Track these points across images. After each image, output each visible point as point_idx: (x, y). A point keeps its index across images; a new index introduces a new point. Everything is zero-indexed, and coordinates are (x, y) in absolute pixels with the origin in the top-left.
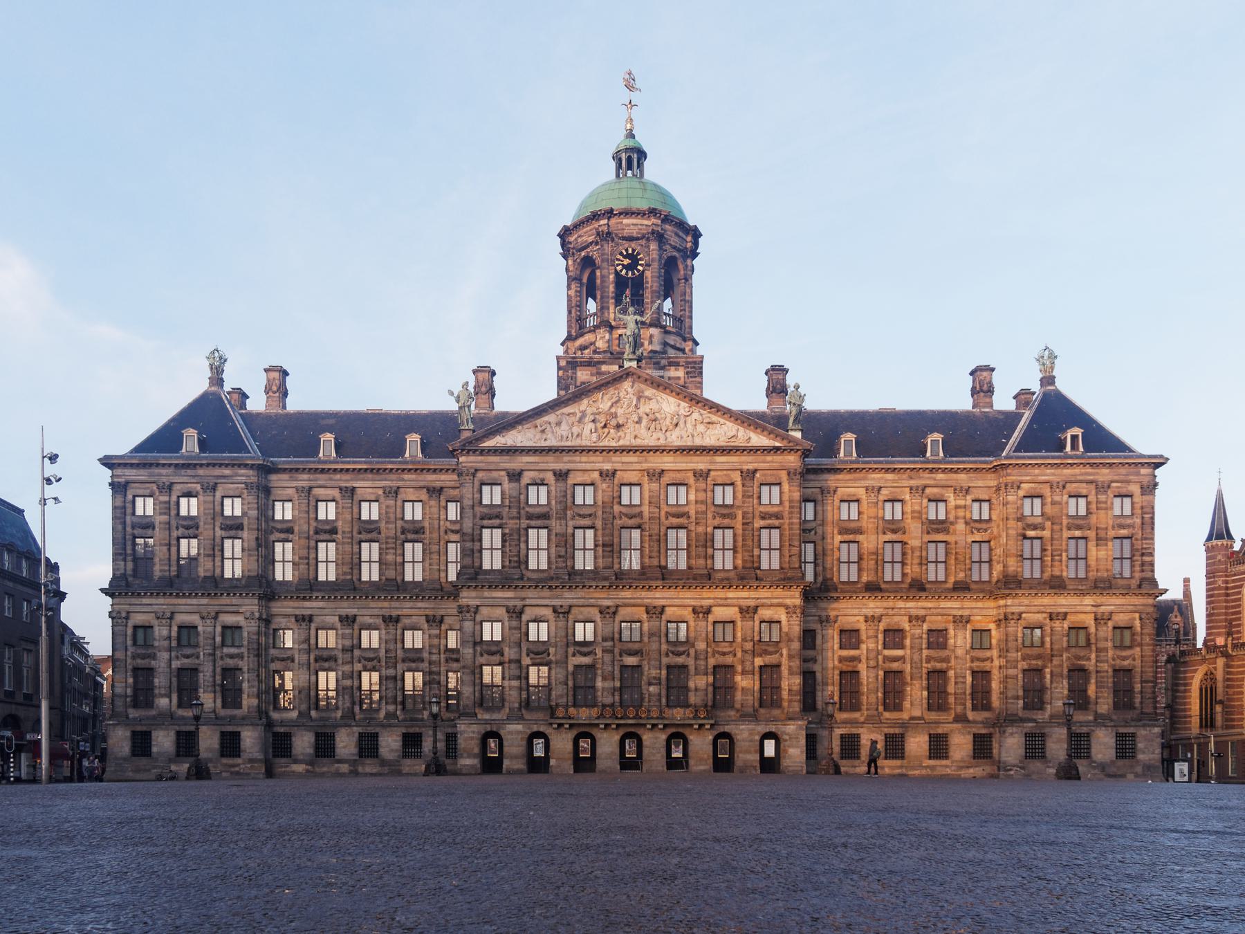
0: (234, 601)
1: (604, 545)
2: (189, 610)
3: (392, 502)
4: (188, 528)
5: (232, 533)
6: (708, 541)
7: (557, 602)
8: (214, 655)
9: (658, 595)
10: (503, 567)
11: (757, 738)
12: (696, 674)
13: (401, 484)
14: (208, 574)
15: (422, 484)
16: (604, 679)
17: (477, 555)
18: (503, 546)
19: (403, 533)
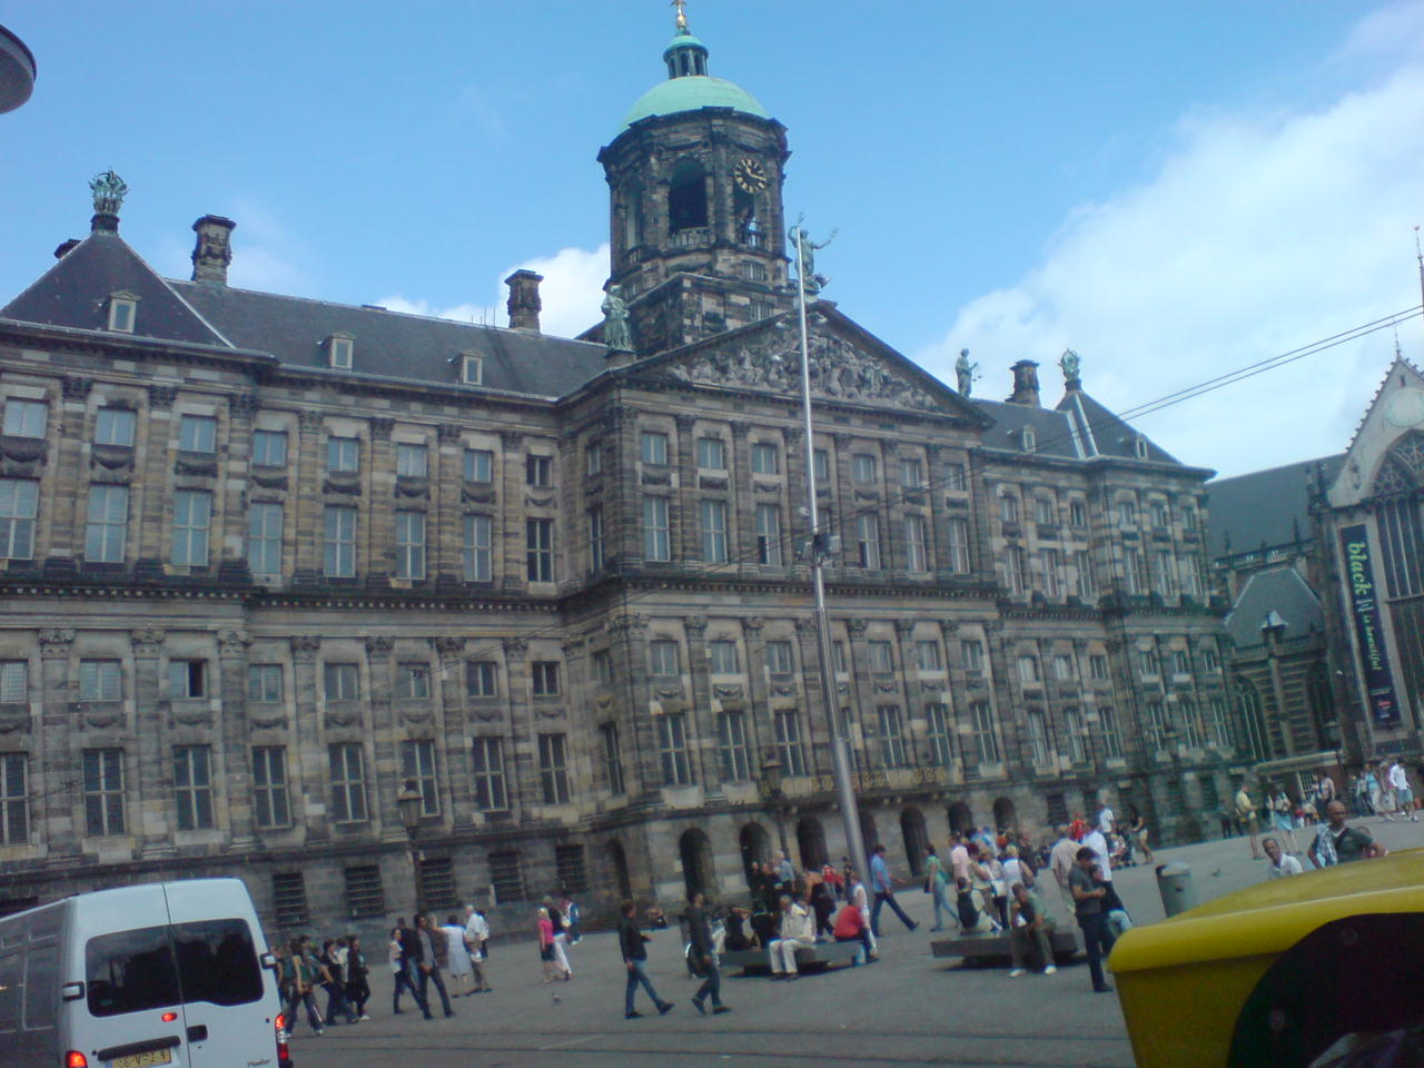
0: (198, 609)
1: (793, 531)
2: (103, 626)
3: (448, 450)
4: (111, 465)
5: (196, 481)
6: (902, 536)
7: (748, 612)
8: (156, 717)
9: (858, 602)
10: (673, 557)
11: (990, 808)
12: (910, 718)
13: (464, 422)
14: (148, 555)
15: (497, 425)
16: (812, 729)
17: (640, 536)
18: (671, 525)
19: (463, 500)
